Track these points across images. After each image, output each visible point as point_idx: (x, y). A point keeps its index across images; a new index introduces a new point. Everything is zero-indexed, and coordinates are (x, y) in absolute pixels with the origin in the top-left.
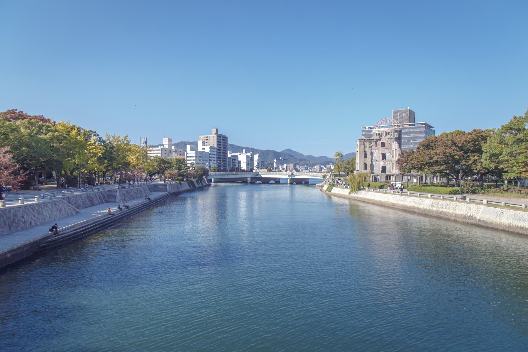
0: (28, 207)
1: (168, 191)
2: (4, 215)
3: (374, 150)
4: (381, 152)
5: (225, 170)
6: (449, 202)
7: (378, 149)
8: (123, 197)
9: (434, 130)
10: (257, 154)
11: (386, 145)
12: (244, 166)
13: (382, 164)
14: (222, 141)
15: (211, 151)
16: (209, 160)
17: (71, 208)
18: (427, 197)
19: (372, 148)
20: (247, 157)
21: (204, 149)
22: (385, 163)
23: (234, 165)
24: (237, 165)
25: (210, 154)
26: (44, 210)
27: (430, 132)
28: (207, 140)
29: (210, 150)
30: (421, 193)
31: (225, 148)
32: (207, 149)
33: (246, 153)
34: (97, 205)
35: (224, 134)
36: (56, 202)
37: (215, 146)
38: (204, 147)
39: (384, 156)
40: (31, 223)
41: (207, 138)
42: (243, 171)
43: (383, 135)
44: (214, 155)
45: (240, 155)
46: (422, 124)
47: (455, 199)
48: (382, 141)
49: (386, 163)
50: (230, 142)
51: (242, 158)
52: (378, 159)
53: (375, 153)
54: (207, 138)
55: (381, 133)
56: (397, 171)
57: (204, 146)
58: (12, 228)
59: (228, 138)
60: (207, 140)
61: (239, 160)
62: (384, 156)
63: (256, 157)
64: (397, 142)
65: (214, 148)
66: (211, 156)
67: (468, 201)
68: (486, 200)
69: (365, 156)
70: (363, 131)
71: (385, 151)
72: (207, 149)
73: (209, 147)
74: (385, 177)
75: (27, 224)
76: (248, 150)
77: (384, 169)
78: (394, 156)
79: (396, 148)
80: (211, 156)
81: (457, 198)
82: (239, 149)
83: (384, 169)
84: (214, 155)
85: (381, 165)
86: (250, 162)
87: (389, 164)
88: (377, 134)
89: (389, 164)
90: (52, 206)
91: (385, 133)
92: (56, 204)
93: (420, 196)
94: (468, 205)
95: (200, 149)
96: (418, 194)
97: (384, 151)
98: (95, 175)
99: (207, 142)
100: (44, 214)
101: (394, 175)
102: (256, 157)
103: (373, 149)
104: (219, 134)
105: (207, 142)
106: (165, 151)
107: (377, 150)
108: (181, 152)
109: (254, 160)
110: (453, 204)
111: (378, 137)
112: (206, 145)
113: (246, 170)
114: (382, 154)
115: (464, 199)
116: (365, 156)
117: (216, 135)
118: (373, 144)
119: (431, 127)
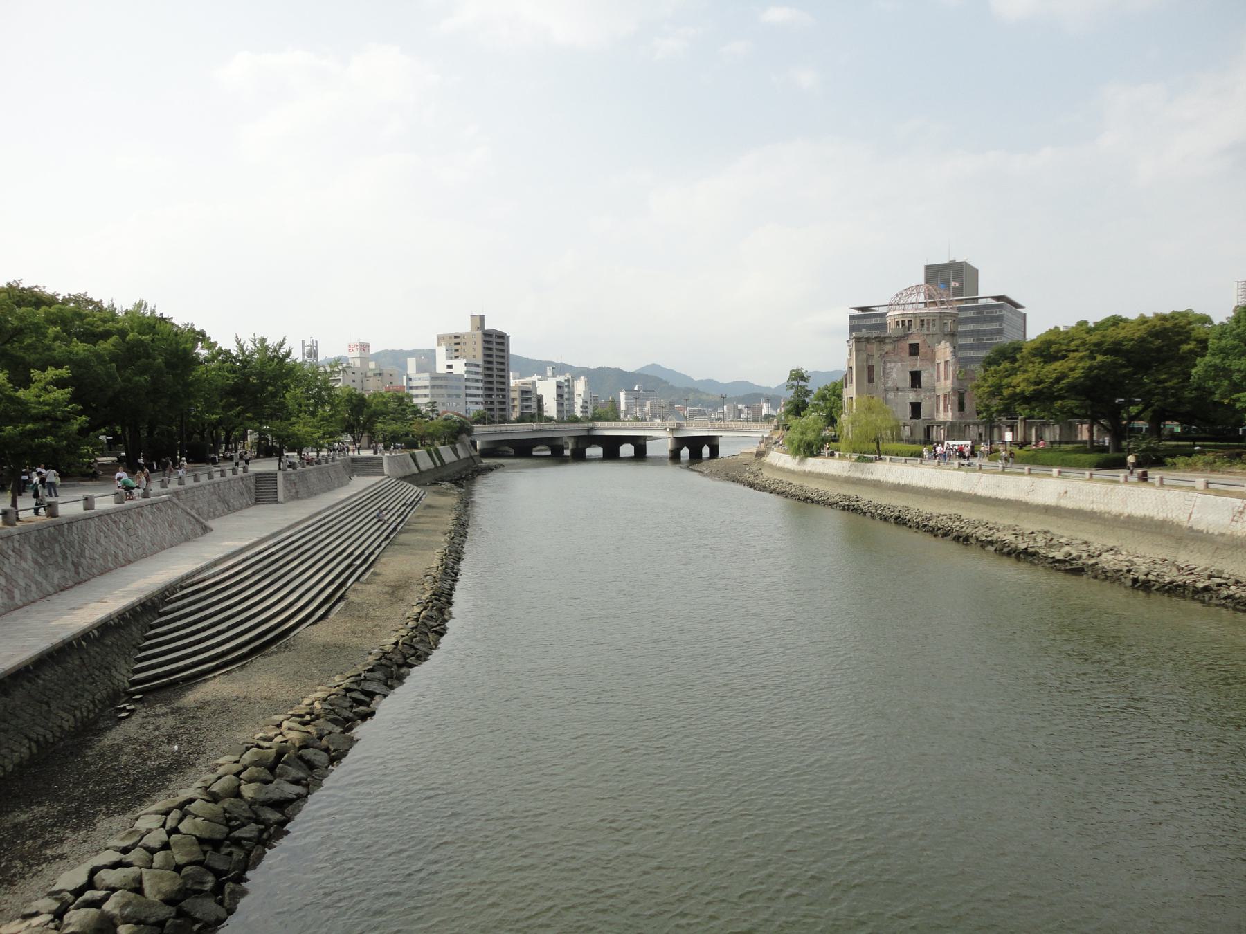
0: (106, 517)
1: (386, 471)
2: (60, 538)
3: (892, 364)
4: (910, 369)
5: (504, 420)
6: (1112, 486)
7: (901, 361)
8: (294, 490)
9: (1025, 315)
10: (582, 378)
11: (921, 350)
12: (551, 408)
13: (912, 397)
14: (494, 346)
15: (467, 372)
16: (463, 396)
17: (191, 519)
18: (1050, 476)
19: (887, 359)
20: (560, 386)
21: (450, 367)
22: (918, 395)
23: (527, 407)
24: (534, 405)
25: (467, 380)
26: (137, 525)
27: (1015, 318)
28: (459, 344)
29: (465, 368)
30: (1032, 468)
31: (503, 364)
32: (460, 367)
33: (554, 375)
34: (237, 510)
35: (501, 328)
36: (160, 504)
37: (479, 360)
38: (450, 362)
39: (916, 378)
40: (116, 556)
41: (458, 341)
42: (550, 419)
43: (913, 326)
44: (477, 381)
45: (539, 380)
46: (998, 298)
47: (1122, 479)
48: (911, 342)
49: (922, 396)
50: (514, 349)
51: (547, 390)
52: (900, 385)
53: (895, 370)
54: (458, 341)
55: (910, 321)
56: (950, 414)
57: (451, 358)
58: (80, 569)
59: (511, 340)
60: (459, 344)
61: (538, 394)
62: (916, 378)
63: (580, 387)
64: (948, 344)
65: (478, 366)
66: (468, 384)
67: (1158, 484)
68: (1203, 479)
69: (871, 380)
70: (852, 317)
71: (918, 364)
72: (460, 367)
73: (465, 361)
74: (923, 430)
75: (109, 558)
76: (559, 369)
77: (916, 409)
78: (943, 378)
79: (948, 359)
80: (468, 384)
81: (1162, 479)
82: (540, 368)
83: (916, 409)
84: (477, 381)
85: (908, 402)
86: (564, 395)
87: (930, 397)
88: (898, 322)
89: (930, 397)
90: (153, 513)
91: (918, 321)
92: (158, 509)
93: (1030, 473)
94: (1157, 494)
95: (441, 369)
96: (1026, 468)
97: (915, 365)
98: (202, 434)
99: (457, 351)
100: (140, 534)
101: (944, 423)
102: (580, 387)
103: (890, 362)
104: (487, 327)
105: (457, 351)
106: (353, 373)
107: (899, 364)
108: (391, 375)
109: (576, 393)
110: (1122, 489)
111: (900, 331)
112: (456, 357)
113: (555, 417)
114: (910, 372)
115: (1144, 478)
116: (871, 380)
117: (480, 332)
118: (888, 348)
119: (1017, 306)
